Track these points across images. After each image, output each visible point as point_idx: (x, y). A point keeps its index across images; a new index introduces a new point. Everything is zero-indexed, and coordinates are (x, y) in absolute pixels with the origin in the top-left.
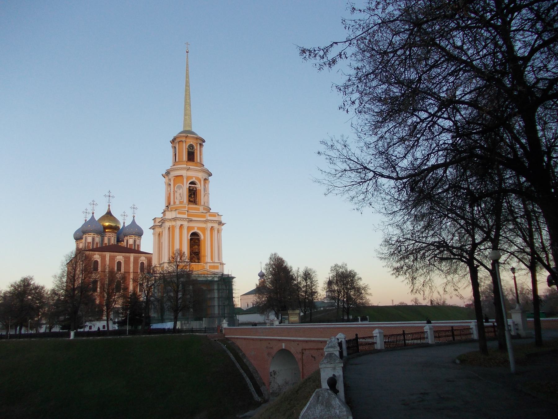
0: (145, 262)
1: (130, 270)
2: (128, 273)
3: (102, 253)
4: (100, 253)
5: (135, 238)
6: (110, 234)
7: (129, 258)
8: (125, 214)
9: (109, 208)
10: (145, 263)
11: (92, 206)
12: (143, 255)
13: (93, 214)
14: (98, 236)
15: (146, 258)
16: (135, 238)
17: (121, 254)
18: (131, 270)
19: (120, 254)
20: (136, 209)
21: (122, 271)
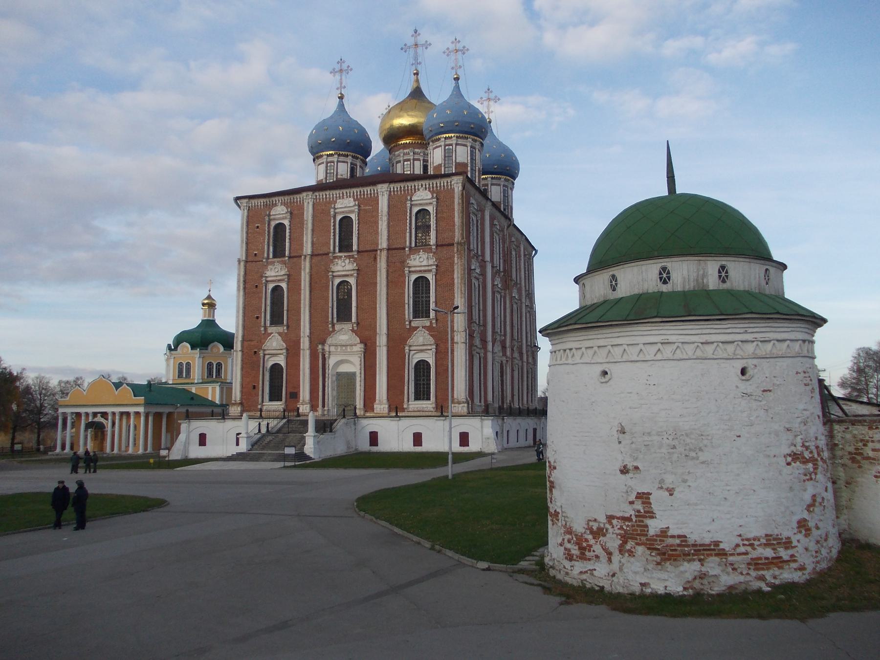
0: (430, 209)
1: (377, 244)
2: (372, 254)
3: (292, 197)
4: (286, 198)
5: (448, 142)
6: (409, 154)
7: (374, 201)
8: (492, 96)
9: (417, 81)
10: (431, 212)
11: (338, 77)
12: (424, 182)
13: (341, 98)
14: (342, 159)
15: (432, 193)
16: (448, 142)
17: (348, 191)
18: (383, 243)
19: (344, 191)
20: (464, 50)
21: (354, 250)
